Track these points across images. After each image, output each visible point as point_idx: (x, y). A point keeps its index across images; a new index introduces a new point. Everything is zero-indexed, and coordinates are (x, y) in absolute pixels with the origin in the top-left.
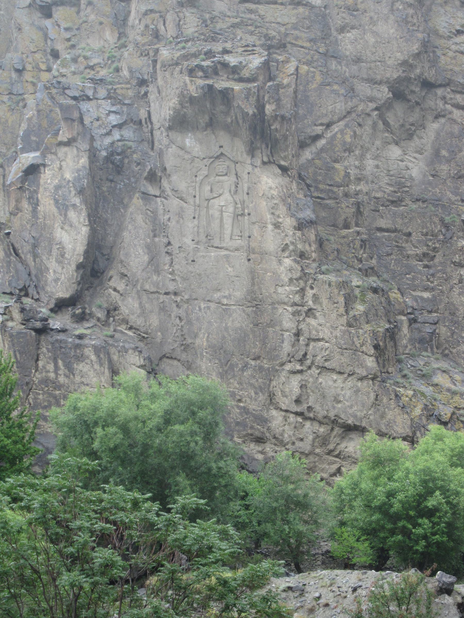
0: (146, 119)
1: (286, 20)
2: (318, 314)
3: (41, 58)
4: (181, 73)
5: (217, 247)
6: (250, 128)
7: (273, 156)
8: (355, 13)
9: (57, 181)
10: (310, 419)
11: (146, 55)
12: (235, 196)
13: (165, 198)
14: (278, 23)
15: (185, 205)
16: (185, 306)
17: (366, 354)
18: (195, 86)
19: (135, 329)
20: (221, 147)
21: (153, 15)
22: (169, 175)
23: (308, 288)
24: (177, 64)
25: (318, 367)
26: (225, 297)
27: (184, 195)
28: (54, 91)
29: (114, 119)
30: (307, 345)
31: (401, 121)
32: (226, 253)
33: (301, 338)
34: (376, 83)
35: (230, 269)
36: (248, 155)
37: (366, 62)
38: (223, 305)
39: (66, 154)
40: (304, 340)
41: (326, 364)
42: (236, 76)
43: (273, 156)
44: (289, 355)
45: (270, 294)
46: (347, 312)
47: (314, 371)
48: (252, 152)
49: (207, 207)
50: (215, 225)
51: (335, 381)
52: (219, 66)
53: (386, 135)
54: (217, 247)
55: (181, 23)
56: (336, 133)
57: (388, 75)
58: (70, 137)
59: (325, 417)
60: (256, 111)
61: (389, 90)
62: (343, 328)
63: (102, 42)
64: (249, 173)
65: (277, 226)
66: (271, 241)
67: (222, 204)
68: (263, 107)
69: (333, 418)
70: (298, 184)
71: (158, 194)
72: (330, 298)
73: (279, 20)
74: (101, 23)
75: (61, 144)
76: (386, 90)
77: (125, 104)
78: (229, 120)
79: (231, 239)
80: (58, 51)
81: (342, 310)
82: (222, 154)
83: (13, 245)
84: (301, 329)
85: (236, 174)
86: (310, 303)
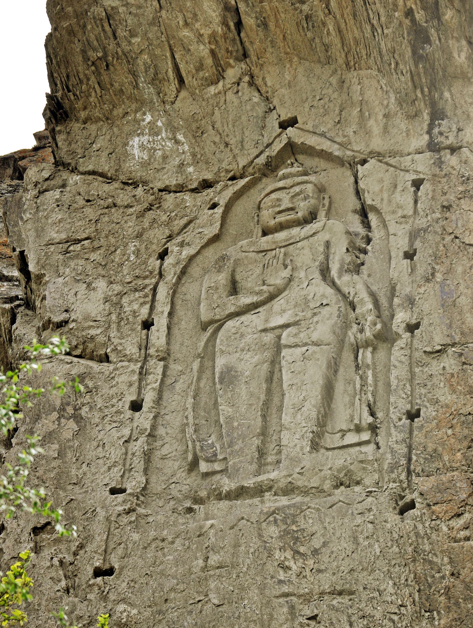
5: (240, 493)
32: (284, 501)
50: (240, 406)
54: (240, 493)
79: (315, 446)
82: (291, 148)
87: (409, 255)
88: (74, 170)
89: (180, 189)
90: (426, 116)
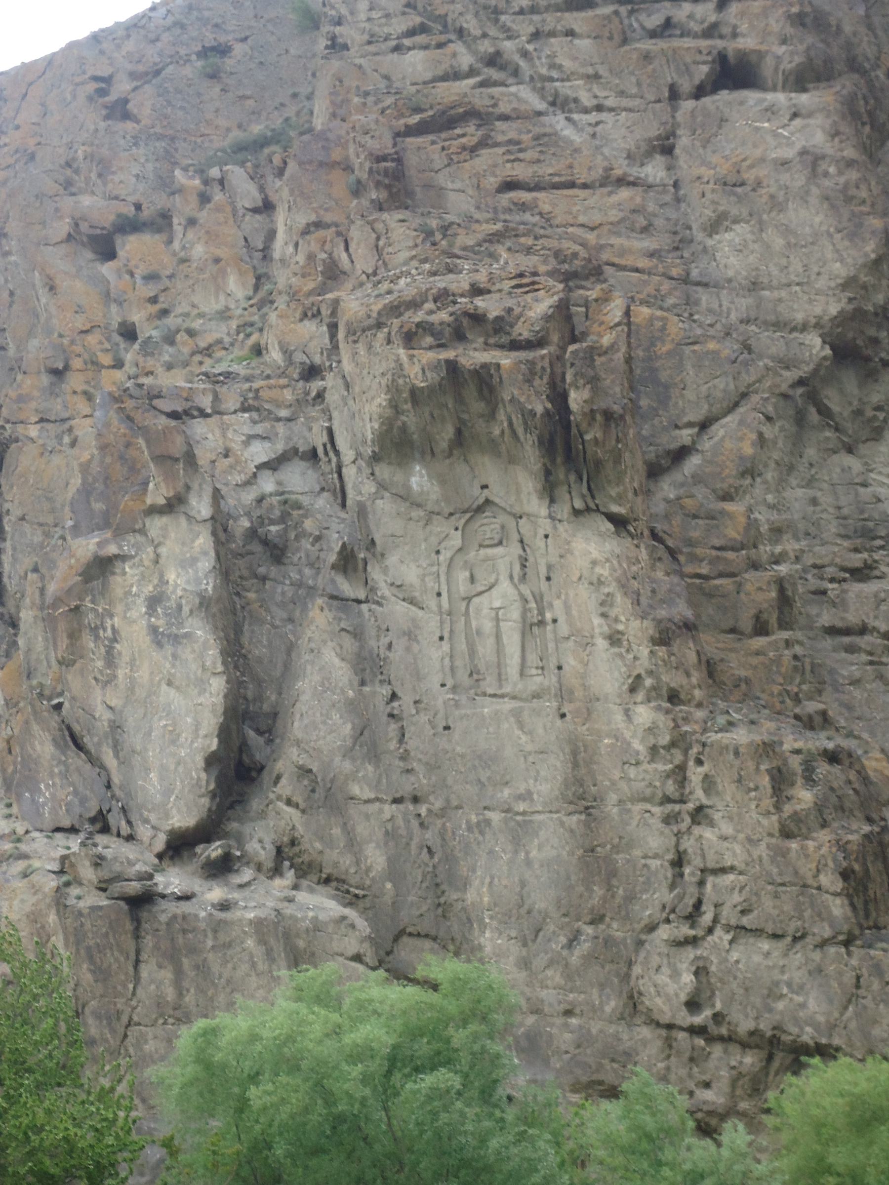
0: (325, 445)
1: (596, 218)
2: (717, 816)
3: (101, 343)
4: (389, 342)
5: (494, 696)
6: (541, 443)
7: (593, 497)
8: (739, 190)
9: (151, 588)
10: (721, 1039)
11: (314, 316)
12: (522, 587)
13: (379, 603)
14: (582, 225)
15: (420, 613)
16: (439, 822)
17: (827, 892)
18: (420, 365)
19: (337, 880)
20: (484, 487)
21: (322, 233)
22: (383, 555)
23: (691, 763)
24: (379, 325)
25: (728, 928)
26: (520, 797)
27: (417, 594)
28: (129, 404)
29: (260, 452)
30: (701, 883)
31: (855, 403)
33: (687, 871)
34: (794, 329)
35: (524, 738)
36: (541, 498)
37: (771, 288)
38: (518, 813)
39: (164, 529)
40: (692, 874)
41: (745, 921)
42: (505, 339)
43: (593, 497)
44: (664, 907)
45: (613, 783)
46: (778, 807)
47: (721, 937)
48: (550, 490)
49: (467, 613)
51: (767, 954)
52: (465, 321)
53: (828, 434)
54: (494, 696)
55: (381, 243)
56: (722, 439)
57: (818, 310)
58: (171, 494)
59: (752, 1033)
60: (549, 406)
61: (824, 342)
62: (774, 841)
63: (222, 297)
64: (546, 536)
65: (614, 639)
66: (606, 674)
67: (497, 604)
68: (564, 396)
69: (769, 1034)
70: (652, 551)
71: (362, 596)
72: (739, 781)
73: (582, 219)
74: (217, 261)
75: (153, 510)
76: (818, 341)
77: (279, 420)
78: (497, 432)
79: (522, 674)
80: (134, 324)
81: (768, 803)
82: (488, 502)
83: (69, 728)
84: (685, 851)
85: (522, 541)
86: (700, 793)
87: (548, 579)
88: (386, 489)
89: (438, 514)
90: (547, 501)
